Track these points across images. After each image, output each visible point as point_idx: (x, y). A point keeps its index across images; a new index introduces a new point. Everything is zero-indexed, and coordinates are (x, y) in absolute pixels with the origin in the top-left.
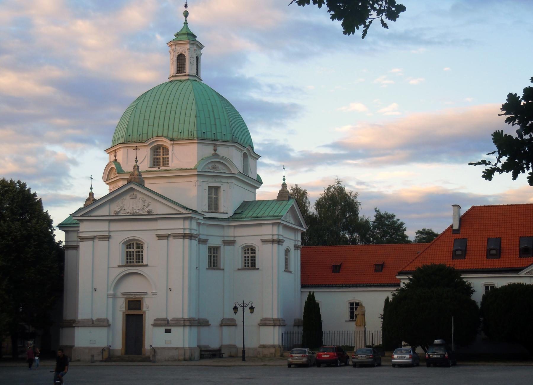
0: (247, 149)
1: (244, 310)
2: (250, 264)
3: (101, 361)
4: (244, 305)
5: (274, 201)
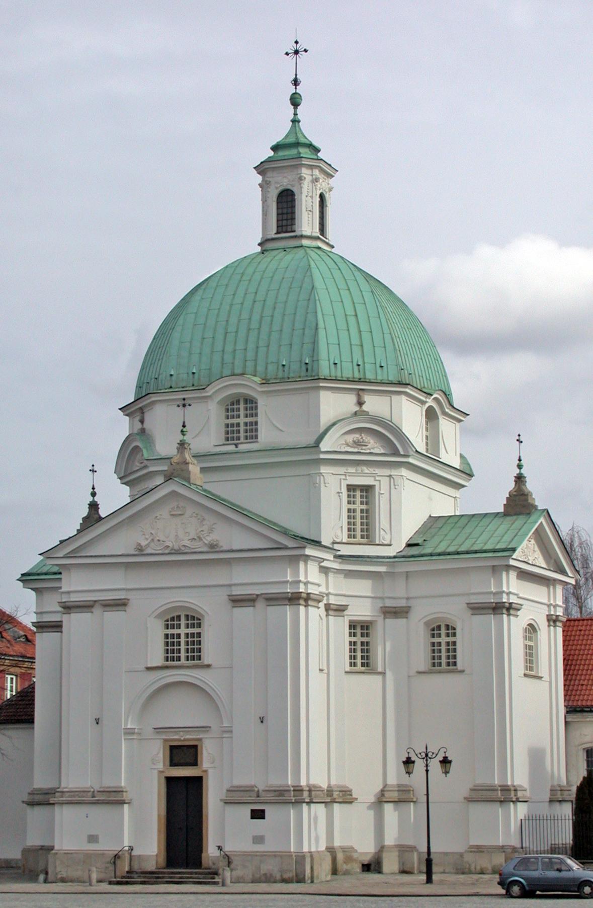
0: (436, 399)
1: (427, 766)
2: (444, 661)
3: (110, 883)
4: (427, 755)
5: (499, 515)
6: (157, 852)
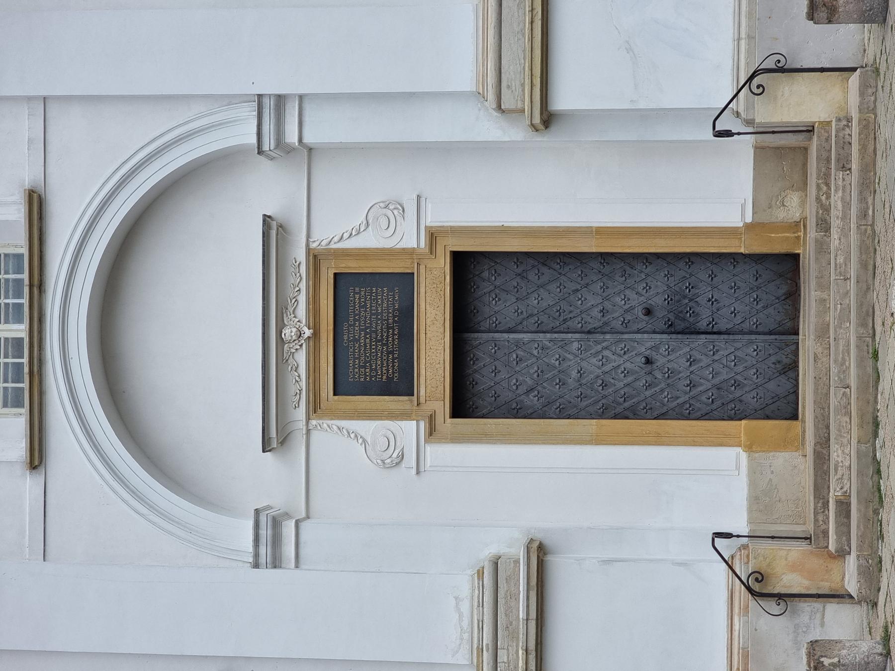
6: (739, 450)
